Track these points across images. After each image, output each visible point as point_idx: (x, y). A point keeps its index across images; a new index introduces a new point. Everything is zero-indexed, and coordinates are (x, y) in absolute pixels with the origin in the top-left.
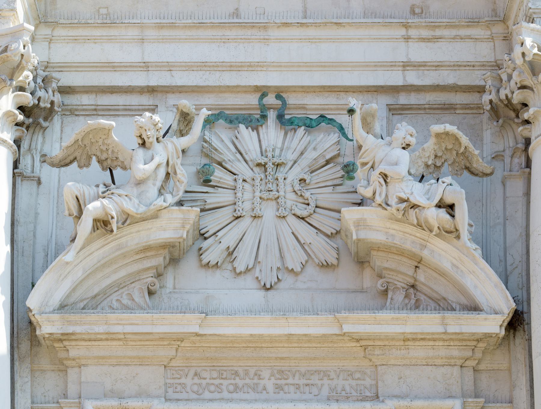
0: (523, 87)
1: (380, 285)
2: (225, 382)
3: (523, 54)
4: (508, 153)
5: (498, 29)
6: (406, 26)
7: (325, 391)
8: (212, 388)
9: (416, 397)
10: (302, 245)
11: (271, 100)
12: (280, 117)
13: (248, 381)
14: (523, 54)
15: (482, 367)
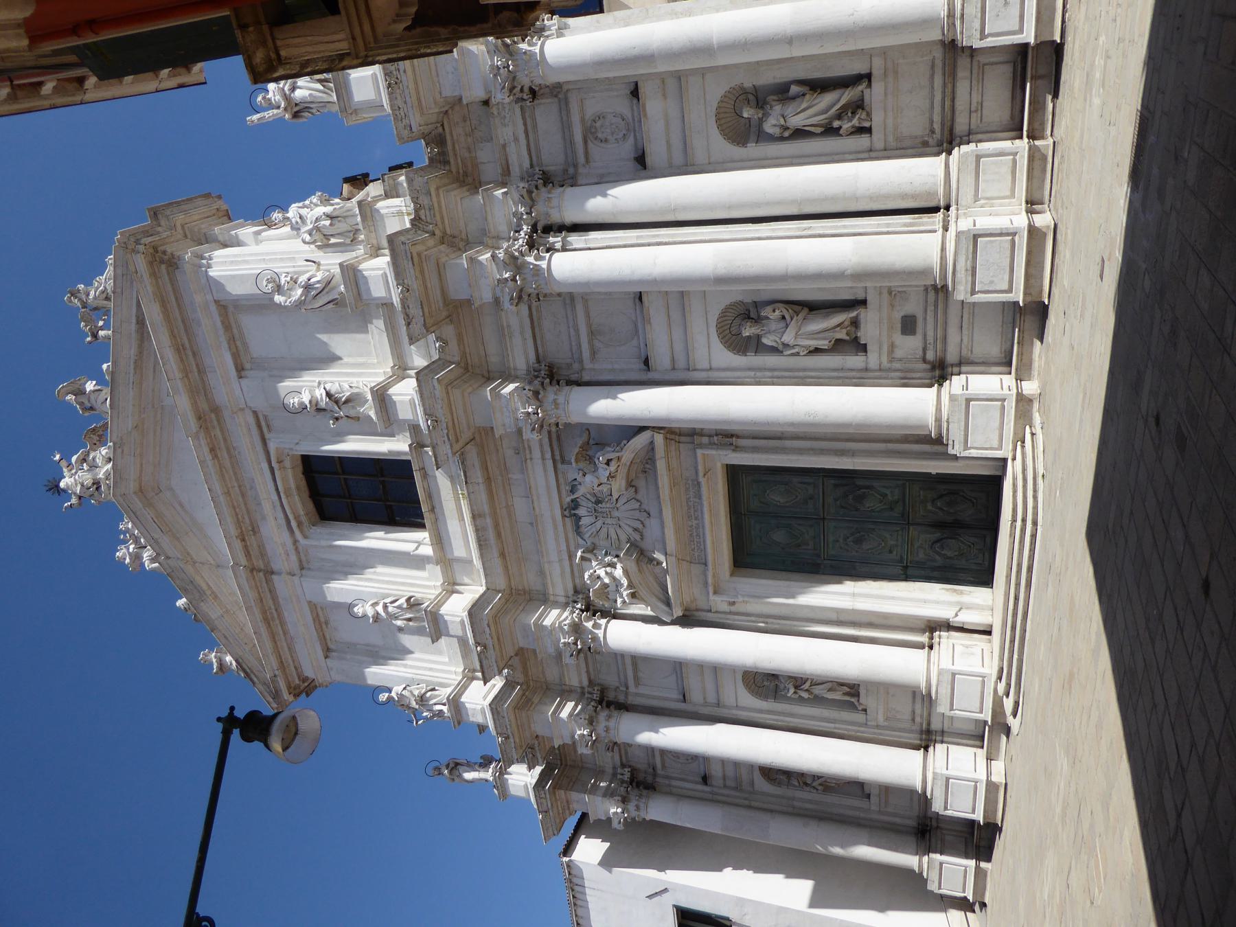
7: (697, 500)
9: (696, 462)
11: (566, 513)
12: (574, 510)
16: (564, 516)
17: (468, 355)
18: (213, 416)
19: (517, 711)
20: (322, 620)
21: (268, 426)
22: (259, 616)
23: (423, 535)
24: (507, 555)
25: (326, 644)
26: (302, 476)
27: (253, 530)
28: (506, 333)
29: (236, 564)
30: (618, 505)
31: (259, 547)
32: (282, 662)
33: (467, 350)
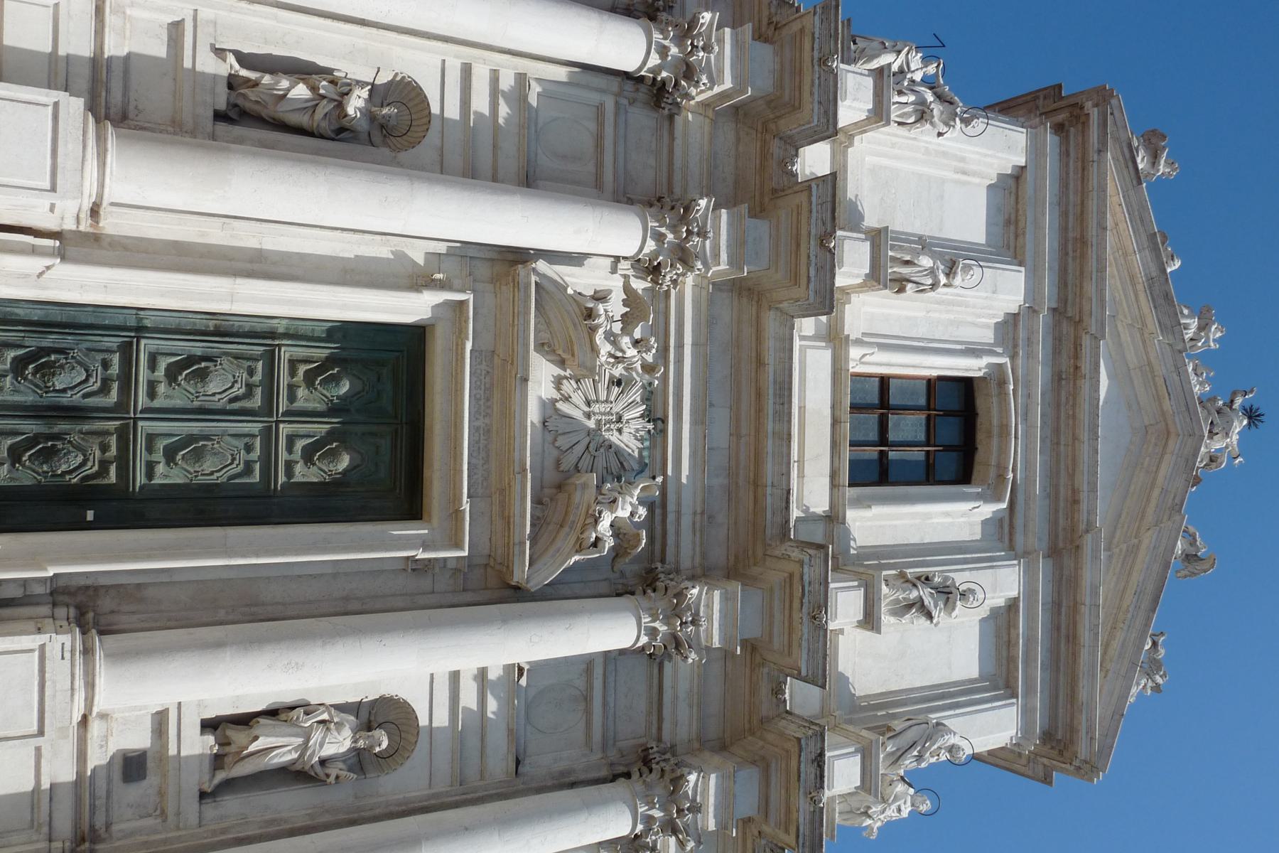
0: (666, 589)
1: (546, 500)
2: (482, 392)
3: (687, 588)
4: (624, 581)
5: (699, 571)
6: (703, 513)
8: (479, 383)
10: (571, 447)
14: (687, 588)
15: (489, 570)
17: (748, 665)
18: (1061, 545)
19: (797, 104)
20: (1012, 228)
21: (1001, 527)
22: (1092, 254)
23: (855, 367)
24: (754, 359)
25: (1017, 188)
26: (979, 447)
27: (1060, 379)
28: (696, 697)
29: (1096, 339)
30: (587, 440)
31: (1060, 352)
32: (1083, 170)
33: (748, 671)
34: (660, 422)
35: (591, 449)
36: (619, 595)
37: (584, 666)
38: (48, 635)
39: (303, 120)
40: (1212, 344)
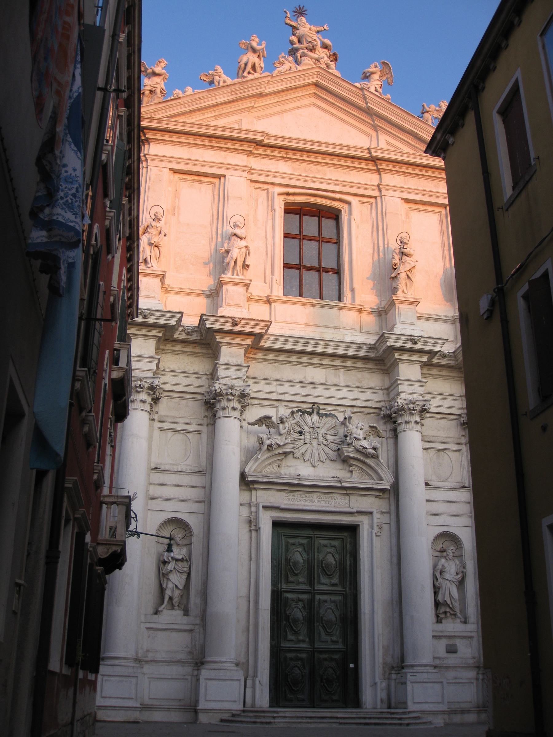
2: (302, 499)
13: (309, 499)
16: (314, 404)
30: (322, 445)
34: (314, 407)
35: (327, 444)
36: (396, 437)
37: (424, 451)
38: (408, 681)
39: (184, 577)
40: (262, 47)
